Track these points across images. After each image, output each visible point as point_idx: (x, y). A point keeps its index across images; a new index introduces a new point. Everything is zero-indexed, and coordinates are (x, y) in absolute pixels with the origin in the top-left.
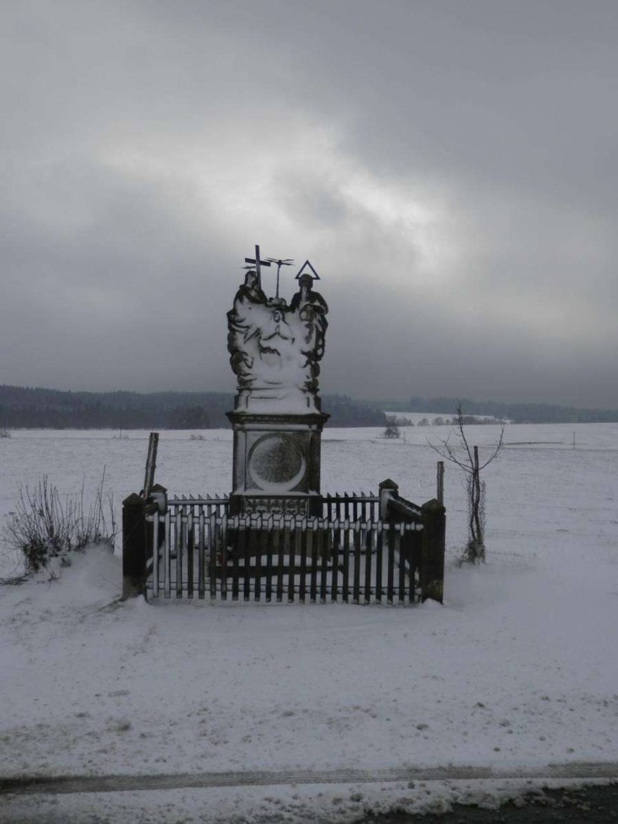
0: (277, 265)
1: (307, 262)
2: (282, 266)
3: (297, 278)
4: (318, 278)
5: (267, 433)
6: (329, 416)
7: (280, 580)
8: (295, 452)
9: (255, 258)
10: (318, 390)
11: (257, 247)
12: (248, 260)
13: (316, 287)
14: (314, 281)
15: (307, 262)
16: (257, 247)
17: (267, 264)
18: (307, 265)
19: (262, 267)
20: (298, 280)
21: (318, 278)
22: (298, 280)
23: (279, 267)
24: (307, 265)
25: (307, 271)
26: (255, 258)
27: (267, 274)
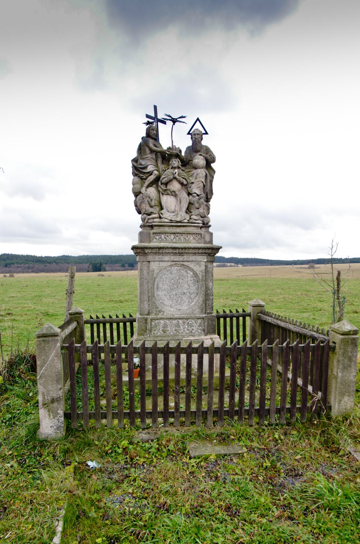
0: (171, 123)
1: (198, 119)
2: (177, 123)
3: (189, 133)
4: (206, 133)
5: (169, 264)
6: (221, 248)
7: (178, 360)
8: (192, 279)
9: (153, 115)
10: (210, 226)
11: (155, 107)
12: (148, 116)
13: (206, 141)
14: (204, 136)
15: (198, 119)
16: (155, 107)
17: (163, 122)
18: (198, 122)
19: (160, 124)
20: (190, 136)
21: (206, 133)
22: (190, 136)
23: (174, 124)
24: (198, 122)
25: (198, 126)
26: (153, 115)
27: (164, 131)
